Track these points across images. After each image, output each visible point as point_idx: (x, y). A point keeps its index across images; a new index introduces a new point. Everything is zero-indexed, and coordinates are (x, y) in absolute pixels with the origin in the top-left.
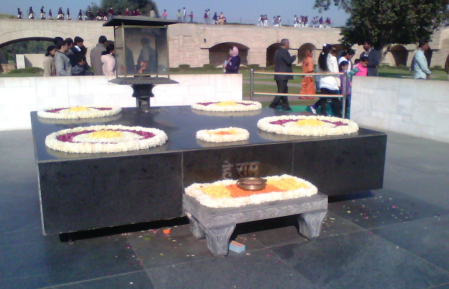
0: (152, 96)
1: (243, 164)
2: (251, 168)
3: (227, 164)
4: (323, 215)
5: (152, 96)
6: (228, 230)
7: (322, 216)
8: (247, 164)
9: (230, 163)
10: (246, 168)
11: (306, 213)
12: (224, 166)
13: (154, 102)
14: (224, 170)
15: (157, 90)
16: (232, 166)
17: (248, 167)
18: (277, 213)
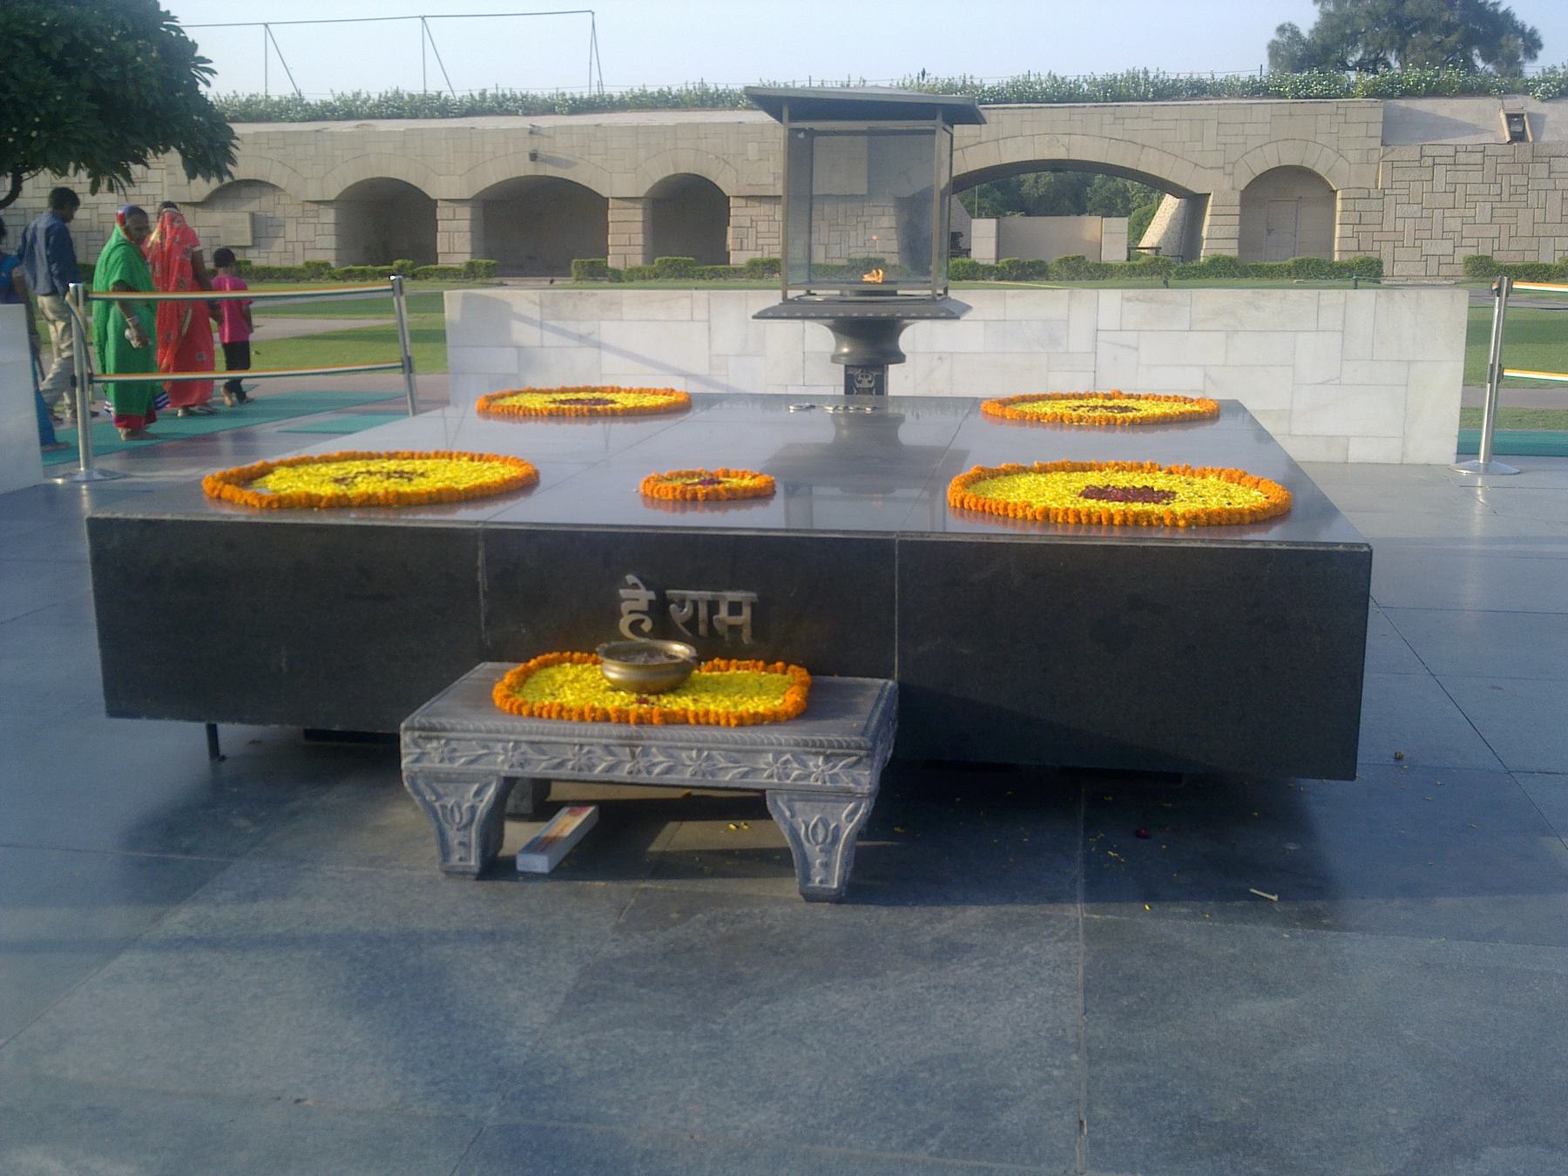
0: (899, 358)
1: (692, 594)
2: (723, 612)
3: (635, 586)
4: (854, 812)
5: (899, 358)
6: (478, 793)
7: (848, 819)
8: (707, 595)
9: (644, 584)
10: (703, 612)
11: (778, 790)
12: (622, 592)
13: (899, 380)
14: (625, 607)
15: (913, 337)
16: (652, 595)
17: (713, 607)
18: (657, 770)
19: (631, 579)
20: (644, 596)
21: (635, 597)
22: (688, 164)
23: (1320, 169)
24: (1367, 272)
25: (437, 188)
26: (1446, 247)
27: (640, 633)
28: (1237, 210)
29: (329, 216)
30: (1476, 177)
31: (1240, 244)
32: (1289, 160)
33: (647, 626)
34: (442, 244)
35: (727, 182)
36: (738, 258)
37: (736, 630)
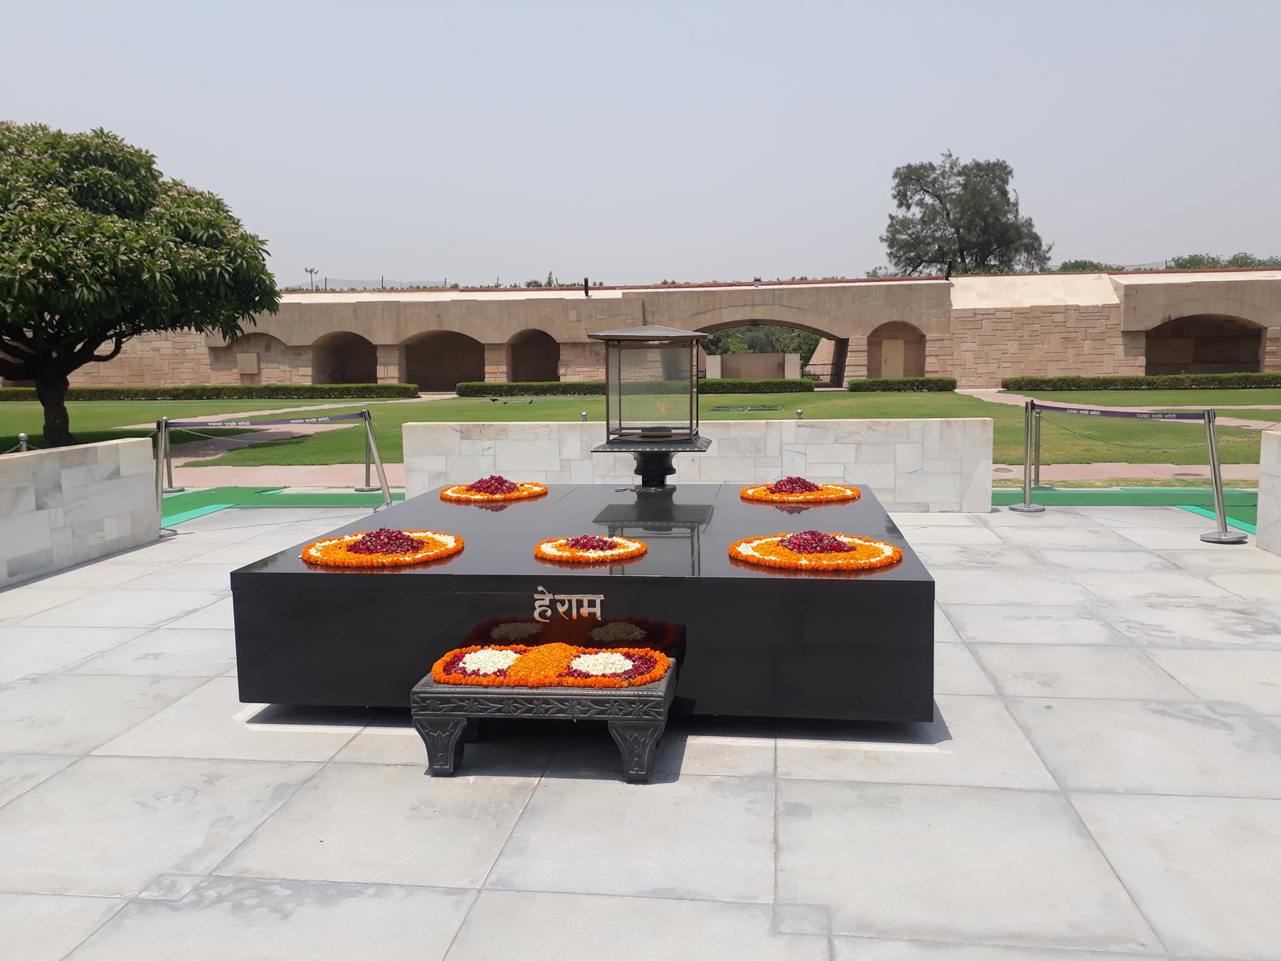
3: (542, 593)
10: (574, 604)
12: (537, 596)
14: (537, 604)
17: (580, 604)
19: (540, 588)
20: (547, 598)
21: (542, 601)
22: (535, 323)
23: (914, 322)
24: (947, 386)
25: (375, 340)
26: (993, 367)
27: (545, 617)
28: (865, 348)
29: (309, 356)
30: (1010, 326)
31: (869, 370)
32: (896, 318)
33: (549, 613)
34: (381, 371)
35: (558, 335)
36: (563, 380)
37: (592, 615)
